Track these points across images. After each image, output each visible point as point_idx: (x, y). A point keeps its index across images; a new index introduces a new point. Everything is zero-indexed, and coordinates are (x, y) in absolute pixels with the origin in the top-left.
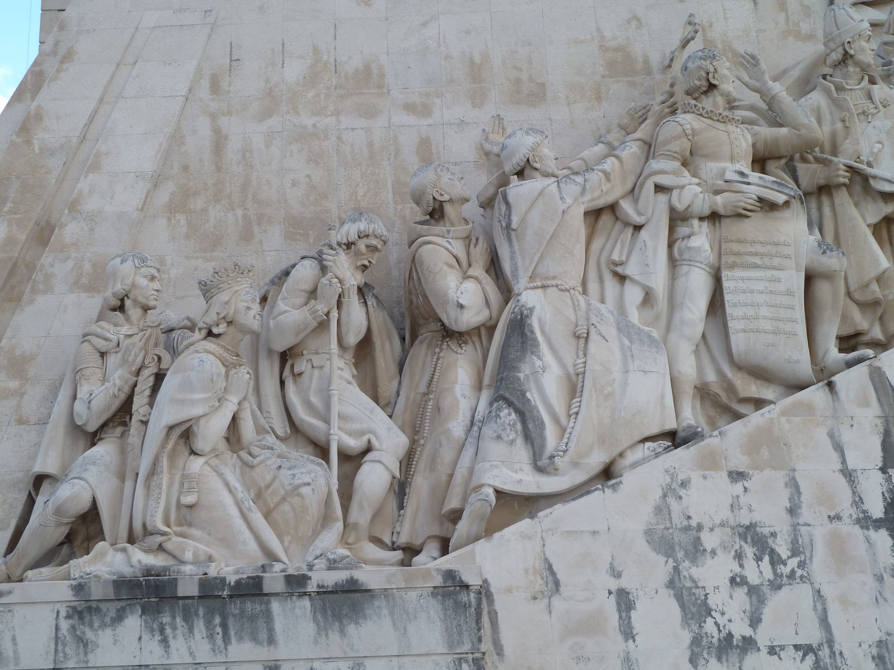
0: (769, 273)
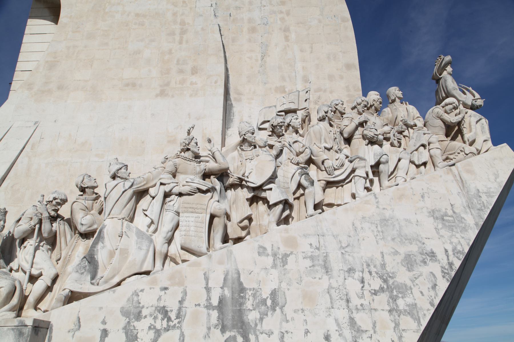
0: (198, 215)
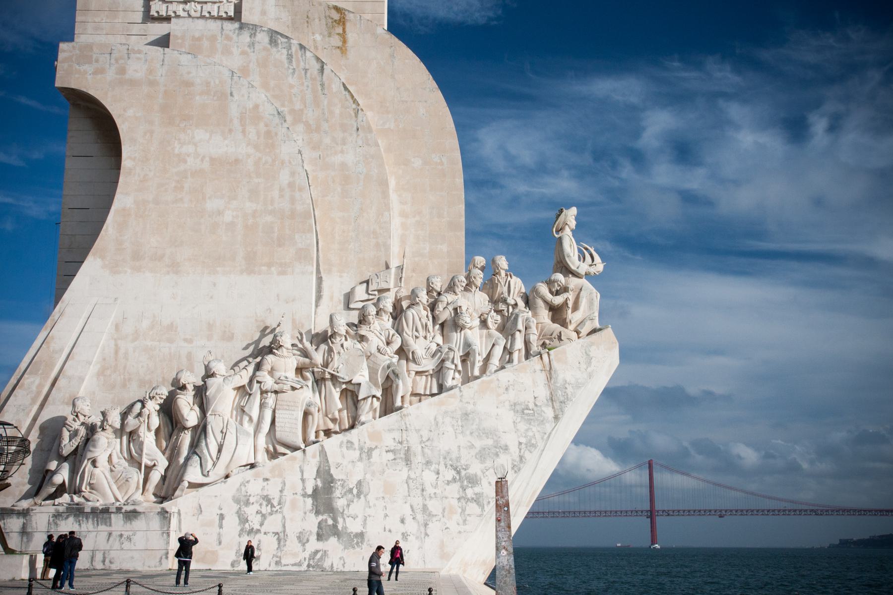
0: (290, 412)
